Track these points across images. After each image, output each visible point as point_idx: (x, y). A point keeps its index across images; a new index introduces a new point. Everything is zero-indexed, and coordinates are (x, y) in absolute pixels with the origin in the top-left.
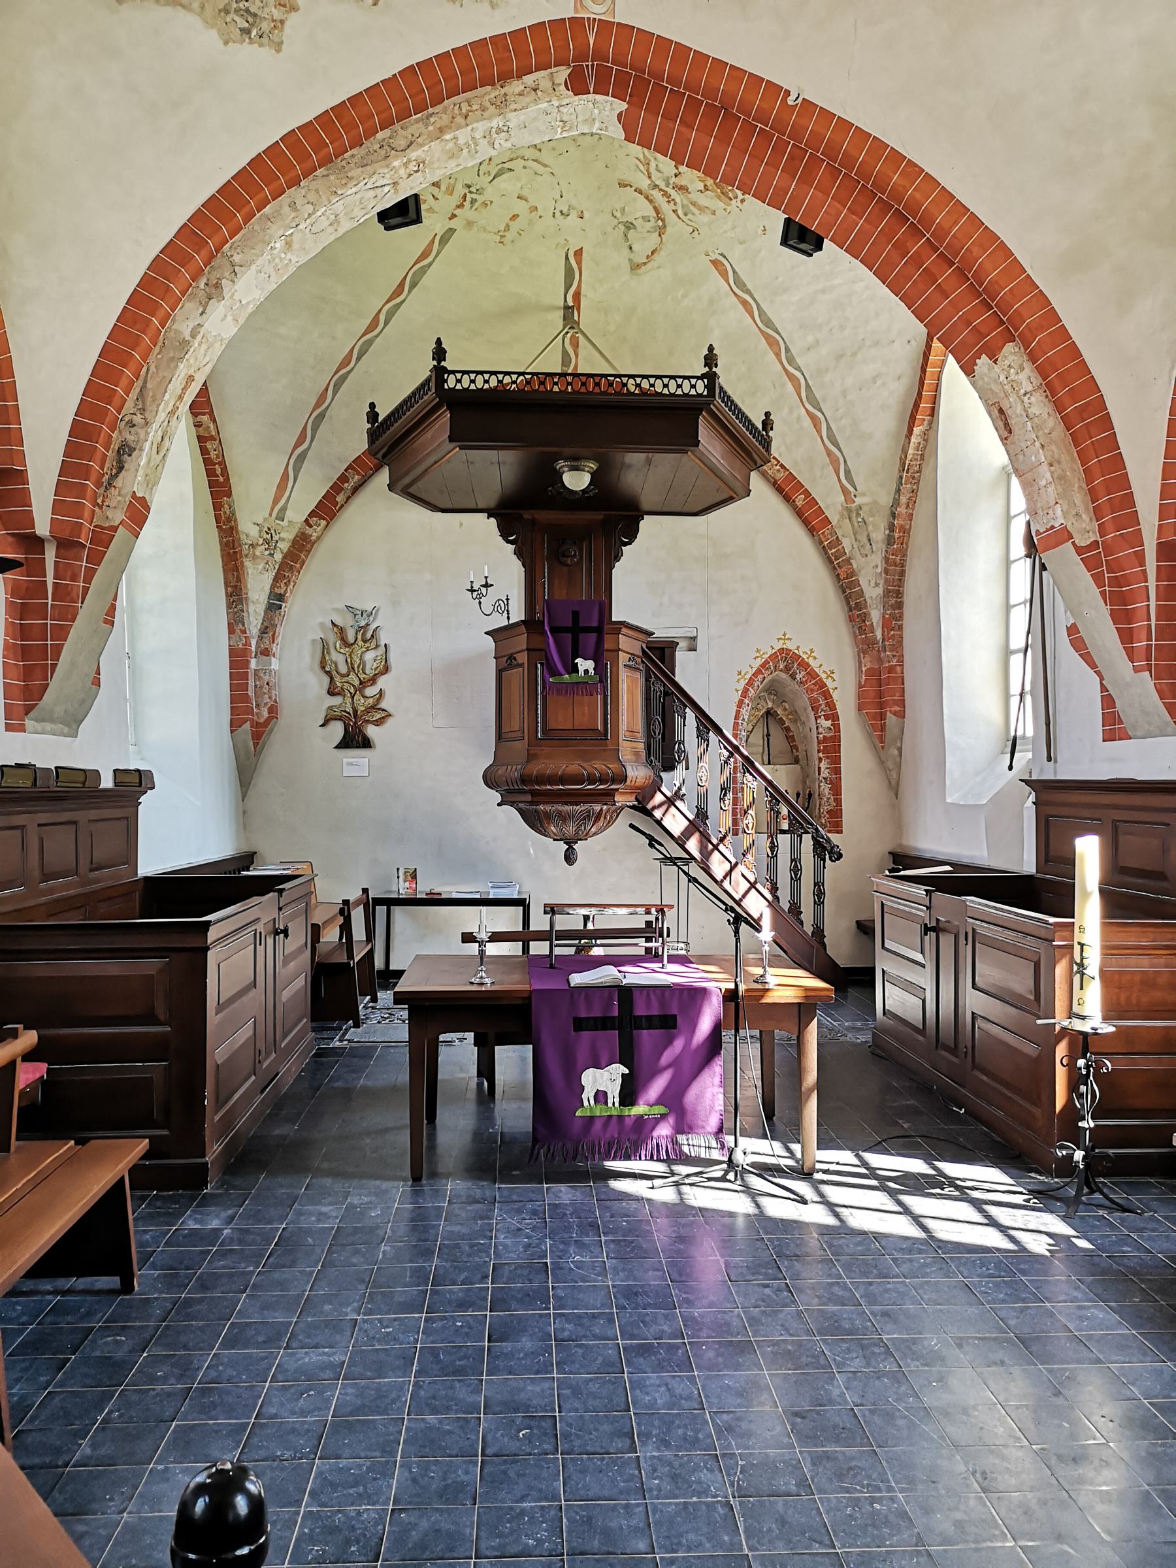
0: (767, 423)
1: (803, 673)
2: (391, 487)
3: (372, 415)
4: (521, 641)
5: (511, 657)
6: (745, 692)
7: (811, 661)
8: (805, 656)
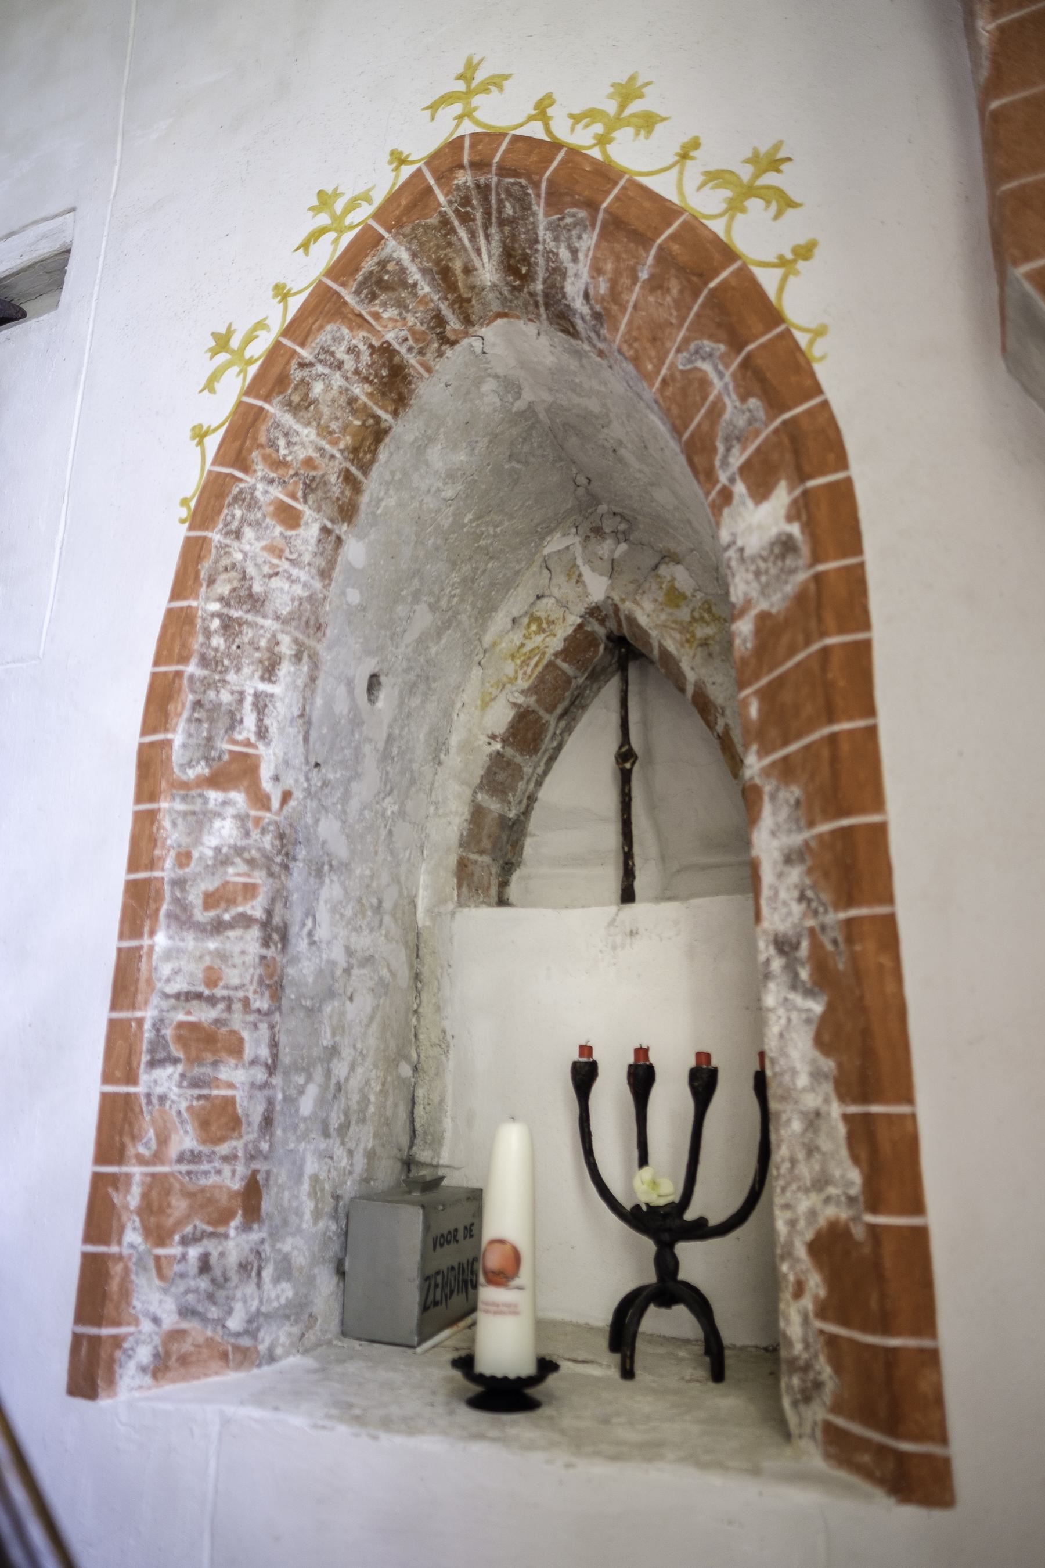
1: (588, 241)
6: (243, 437)
7: (633, 155)
8: (582, 138)
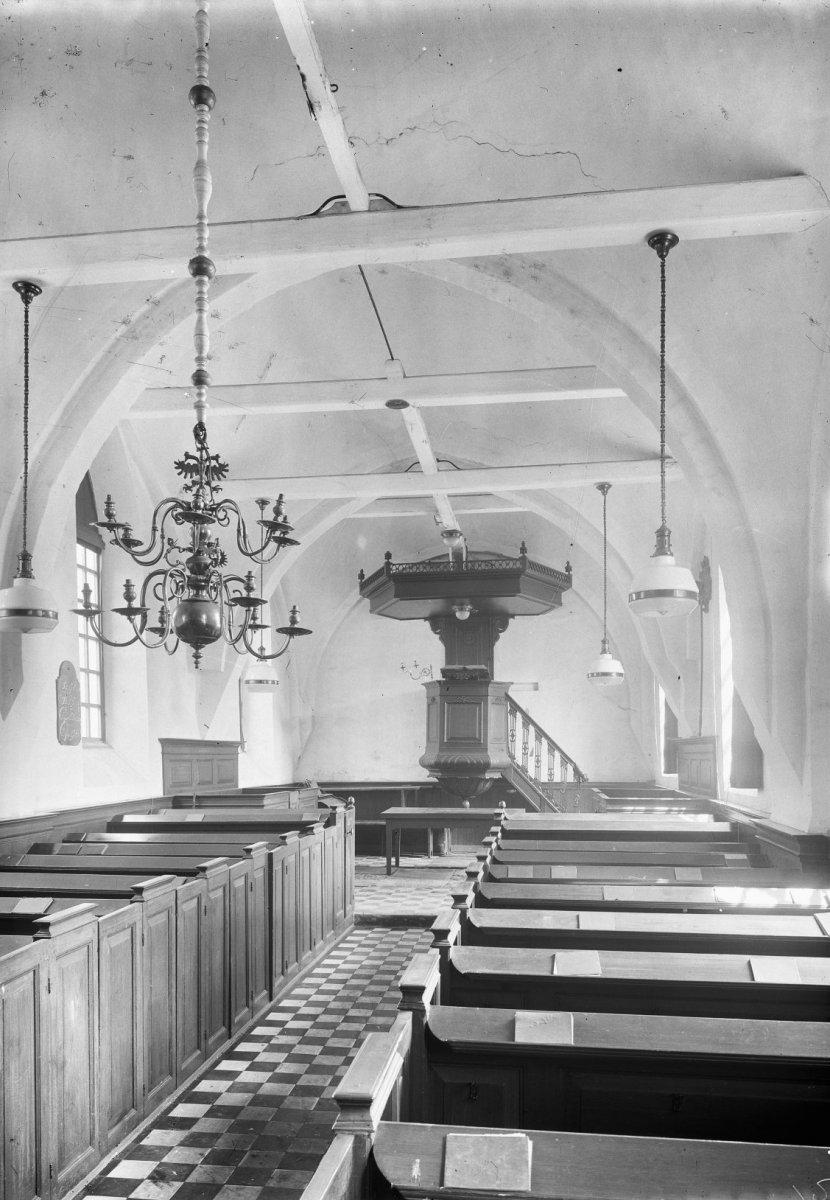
0: (568, 569)
2: (371, 611)
3: (361, 576)
4: (437, 691)
5: (434, 699)
